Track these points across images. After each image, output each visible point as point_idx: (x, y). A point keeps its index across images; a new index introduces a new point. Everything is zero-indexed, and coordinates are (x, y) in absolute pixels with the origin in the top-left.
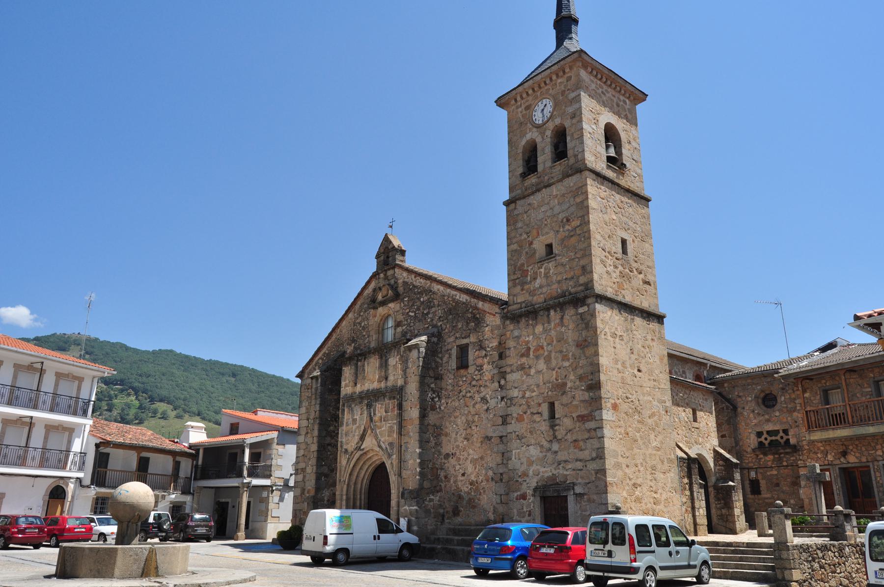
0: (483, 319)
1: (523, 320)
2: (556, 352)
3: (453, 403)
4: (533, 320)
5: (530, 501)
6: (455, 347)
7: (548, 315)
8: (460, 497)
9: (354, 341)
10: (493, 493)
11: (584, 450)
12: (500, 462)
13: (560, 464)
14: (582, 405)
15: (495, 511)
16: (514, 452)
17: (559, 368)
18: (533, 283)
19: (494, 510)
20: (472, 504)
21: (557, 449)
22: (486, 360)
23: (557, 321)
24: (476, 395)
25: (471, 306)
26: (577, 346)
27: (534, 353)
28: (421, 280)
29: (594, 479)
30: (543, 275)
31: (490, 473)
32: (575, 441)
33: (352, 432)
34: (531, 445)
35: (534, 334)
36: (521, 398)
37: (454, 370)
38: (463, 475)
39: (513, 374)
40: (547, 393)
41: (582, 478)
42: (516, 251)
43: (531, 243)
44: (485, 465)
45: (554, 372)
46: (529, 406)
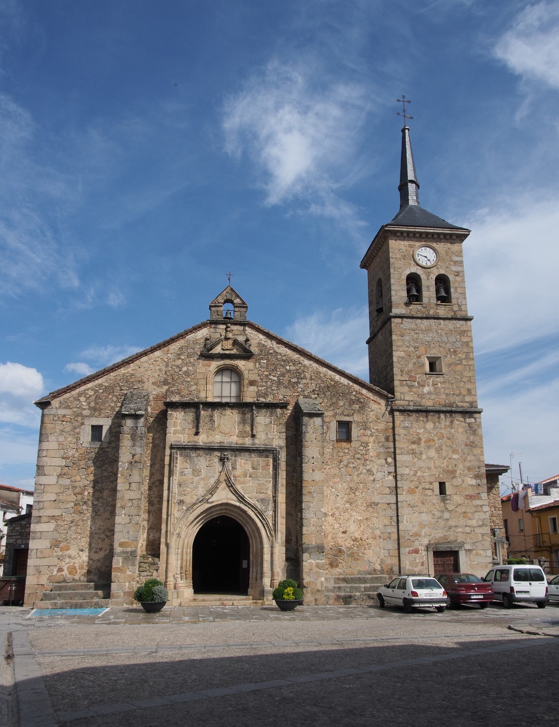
0: (366, 404)
1: (414, 415)
2: (447, 446)
3: (332, 470)
4: (423, 417)
5: (423, 555)
6: (335, 421)
7: (439, 417)
8: (340, 551)
9: (165, 383)
10: (380, 548)
11: (472, 519)
12: (388, 524)
13: (451, 528)
14: (470, 487)
15: (382, 561)
16: (405, 517)
17: (450, 459)
18: (421, 388)
19: (382, 562)
20: (354, 556)
21: (448, 517)
22: (371, 439)
23: (448, 423)
24: (361, 467)
25: (354, 391)
26: (466, 445)
27: (425, 442)
28: (287, 349)
29: (480, 538)
30: (431, 386)
31: (378, 532)
32: (464, 512)
33: (192, 483)
34: (423, 512)
35: (425, 428)
36: (412, 475)
37: (333, 441)
38: (344, 532)
39: (403, 455)
40: (439, 475)
41: (471, 538)
42: (402, 358)
43: (419, 357)
44: (371, 525)
45: (445, 461)
46: (420, 483)
